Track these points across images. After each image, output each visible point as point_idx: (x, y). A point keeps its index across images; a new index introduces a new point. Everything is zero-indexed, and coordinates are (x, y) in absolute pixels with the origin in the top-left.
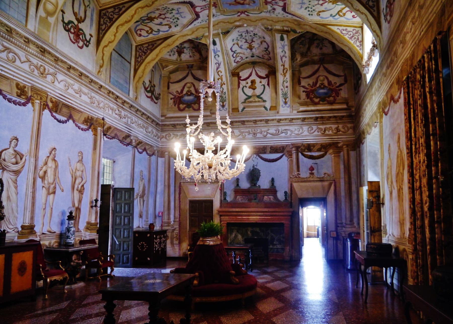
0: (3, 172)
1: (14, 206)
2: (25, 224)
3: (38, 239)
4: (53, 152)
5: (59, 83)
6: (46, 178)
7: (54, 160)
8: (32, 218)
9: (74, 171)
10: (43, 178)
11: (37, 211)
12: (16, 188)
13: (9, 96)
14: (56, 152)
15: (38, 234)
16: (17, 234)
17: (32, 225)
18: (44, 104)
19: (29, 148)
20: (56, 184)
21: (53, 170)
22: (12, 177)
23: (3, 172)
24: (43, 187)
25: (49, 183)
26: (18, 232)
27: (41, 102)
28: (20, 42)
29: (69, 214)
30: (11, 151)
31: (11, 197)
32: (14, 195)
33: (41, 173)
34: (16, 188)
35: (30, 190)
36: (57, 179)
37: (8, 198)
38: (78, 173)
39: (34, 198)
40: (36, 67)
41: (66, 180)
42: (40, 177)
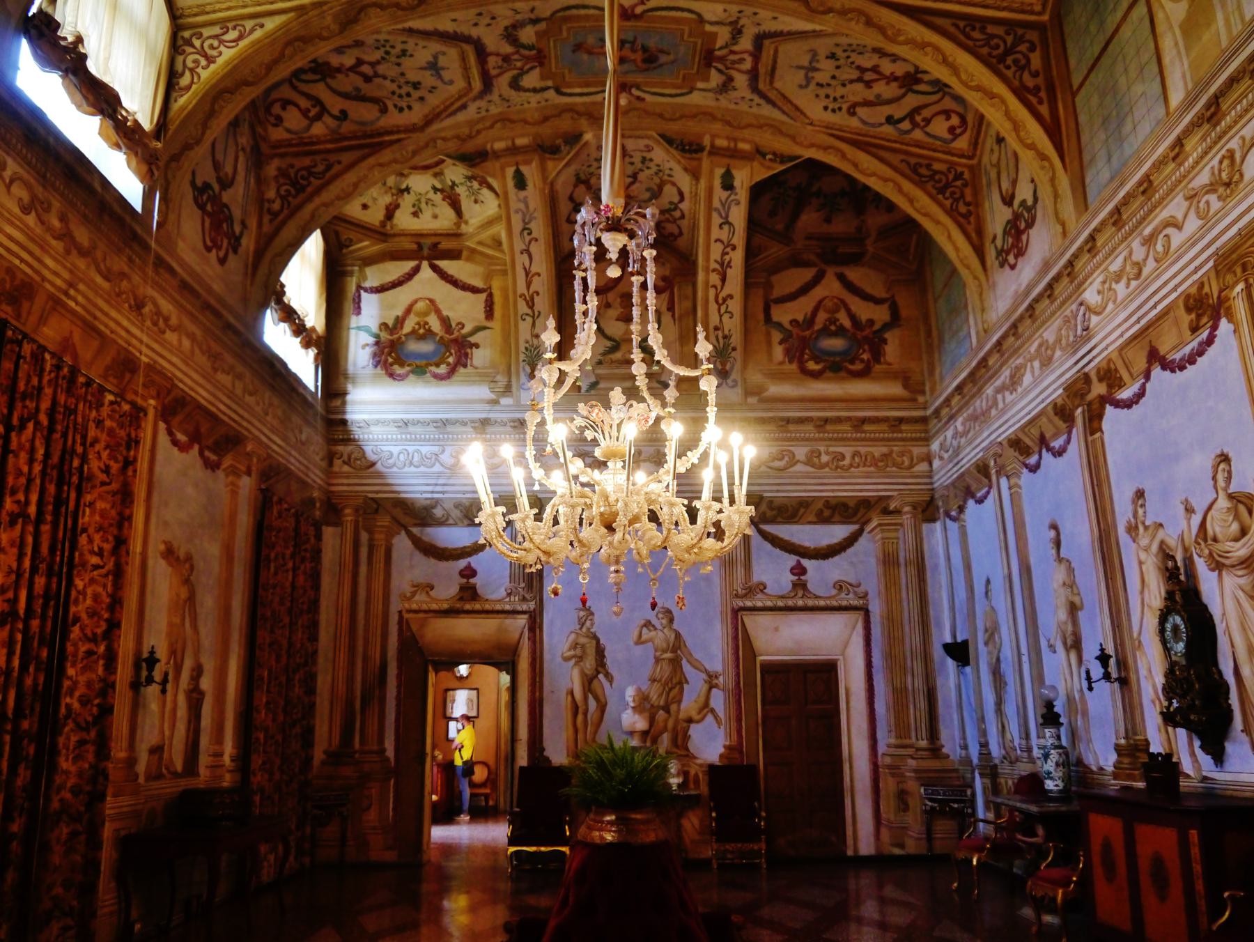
0: (1220, 575)
22: (1242, 581)
23: (1220, 575)
28: (1169, 177)
30: (1223, 503)
40: (1211, 188)
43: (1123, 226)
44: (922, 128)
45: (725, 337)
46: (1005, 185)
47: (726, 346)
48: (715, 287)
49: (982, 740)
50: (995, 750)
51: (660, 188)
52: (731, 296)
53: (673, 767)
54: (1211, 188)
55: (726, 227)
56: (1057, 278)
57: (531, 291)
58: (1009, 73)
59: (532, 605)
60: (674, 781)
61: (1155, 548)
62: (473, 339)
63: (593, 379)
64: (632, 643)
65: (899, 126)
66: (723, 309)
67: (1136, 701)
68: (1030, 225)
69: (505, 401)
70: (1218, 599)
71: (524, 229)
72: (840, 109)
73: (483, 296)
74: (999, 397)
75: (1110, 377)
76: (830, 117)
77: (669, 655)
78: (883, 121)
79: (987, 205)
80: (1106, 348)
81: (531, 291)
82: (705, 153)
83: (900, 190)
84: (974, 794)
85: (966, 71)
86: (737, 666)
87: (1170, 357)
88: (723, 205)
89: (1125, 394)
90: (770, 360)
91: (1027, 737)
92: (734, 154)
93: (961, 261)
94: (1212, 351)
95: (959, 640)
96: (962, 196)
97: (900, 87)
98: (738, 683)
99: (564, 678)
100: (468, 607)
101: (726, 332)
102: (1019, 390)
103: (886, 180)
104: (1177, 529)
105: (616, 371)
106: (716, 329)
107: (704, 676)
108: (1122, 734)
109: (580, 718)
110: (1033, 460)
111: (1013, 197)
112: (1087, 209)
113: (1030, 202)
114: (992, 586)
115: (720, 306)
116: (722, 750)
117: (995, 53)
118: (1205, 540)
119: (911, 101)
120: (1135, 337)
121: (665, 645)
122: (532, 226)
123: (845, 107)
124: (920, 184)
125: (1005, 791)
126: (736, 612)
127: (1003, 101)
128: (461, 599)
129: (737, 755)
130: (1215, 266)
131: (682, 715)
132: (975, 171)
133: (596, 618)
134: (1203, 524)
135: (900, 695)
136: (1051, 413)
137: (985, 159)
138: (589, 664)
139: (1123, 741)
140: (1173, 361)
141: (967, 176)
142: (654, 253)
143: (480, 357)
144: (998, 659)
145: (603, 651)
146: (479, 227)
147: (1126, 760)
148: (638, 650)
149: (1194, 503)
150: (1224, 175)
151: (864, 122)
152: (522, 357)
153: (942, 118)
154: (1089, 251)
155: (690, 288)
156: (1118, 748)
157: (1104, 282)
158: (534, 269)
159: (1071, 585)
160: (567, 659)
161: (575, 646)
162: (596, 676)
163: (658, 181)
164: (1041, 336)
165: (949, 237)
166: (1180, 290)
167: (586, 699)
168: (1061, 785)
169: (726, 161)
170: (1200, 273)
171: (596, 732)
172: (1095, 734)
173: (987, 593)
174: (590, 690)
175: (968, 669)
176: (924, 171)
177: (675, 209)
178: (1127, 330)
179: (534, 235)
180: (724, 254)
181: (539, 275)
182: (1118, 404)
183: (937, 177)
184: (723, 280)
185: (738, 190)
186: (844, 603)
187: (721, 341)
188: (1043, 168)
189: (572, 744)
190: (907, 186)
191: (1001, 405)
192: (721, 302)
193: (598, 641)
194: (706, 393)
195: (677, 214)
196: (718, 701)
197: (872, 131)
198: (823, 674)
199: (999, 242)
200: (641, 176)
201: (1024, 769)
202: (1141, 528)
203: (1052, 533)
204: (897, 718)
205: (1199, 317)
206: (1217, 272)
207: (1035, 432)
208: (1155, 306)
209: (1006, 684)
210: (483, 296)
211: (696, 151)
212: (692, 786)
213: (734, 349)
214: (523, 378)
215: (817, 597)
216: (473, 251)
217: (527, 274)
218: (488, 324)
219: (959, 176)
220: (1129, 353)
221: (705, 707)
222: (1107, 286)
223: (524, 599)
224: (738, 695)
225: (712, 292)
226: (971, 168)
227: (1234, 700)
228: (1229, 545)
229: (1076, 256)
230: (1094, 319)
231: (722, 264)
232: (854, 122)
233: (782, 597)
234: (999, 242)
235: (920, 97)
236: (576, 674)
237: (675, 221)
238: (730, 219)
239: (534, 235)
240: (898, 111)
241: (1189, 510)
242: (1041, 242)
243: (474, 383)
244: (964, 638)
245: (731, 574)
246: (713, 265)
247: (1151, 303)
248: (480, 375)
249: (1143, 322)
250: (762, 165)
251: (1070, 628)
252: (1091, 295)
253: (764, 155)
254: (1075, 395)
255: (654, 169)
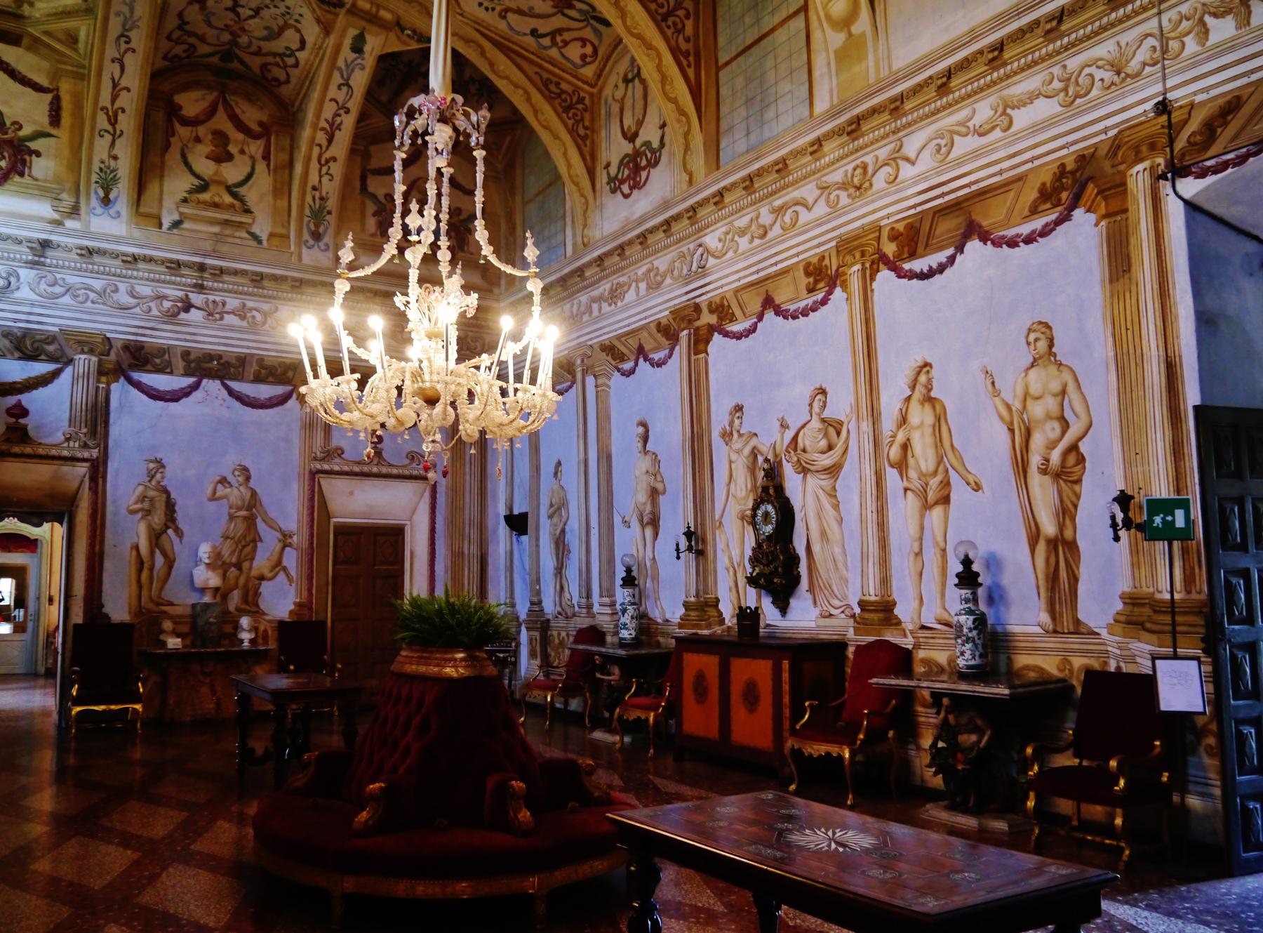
0: (805, 478)
1: (837, 551)
2: (867, 598)
3: (907, 642)
4: (923, 378)
5: (913, 163)
6: (911, 461)
7: (929, 400)
8: (885, 581)
9: (1017, 405)
10: (901, 466)
11: (895, 560)
12: (836, 507)
13: (792, 308)
14: (934, 373)
15: (909, 626)
16: (851, 621)
17: (888, 602)
18: (873, 263)
19: (851, 398)
20: (947, 471)
21: (929, 431)
22: (823, 483)
23: (805, 478)
24: (906, 490)
25: (922, 475)
26: (853, 616)
27: (863, 264)
28: (805, 166)
29: (960, 568)
30: (816, 424)
31: (828, 531)
32: (834, 525)
33: (895, 452)
34: (836, 507)
35: (871, 505)
36: (950, 454)
37: (823, 534)
38: (1037, 410)
39: (882, 525)
40: (843, 186)
41: (986, 446)
42: (892, 466)
43: (754, 192)
44: (559, 48)
45: (322, 199)
46: (628, 122)
47: (322, 208)
48: (320, 146)
49: (535, 599)
50: (549, 606)
51: (282, 30)
52: (334, 159)
53: (245, 622)
54: (843, 186)
55: (345, 89)
56: (676, 218)
57: (116, 106)
58: (669, 32)
59: (95, 453)
60: (246, 636)
61: (747, 451)
62: (33, 145)
63: (176, 217)
64: (205, 499)
65: (541, 40)
66: (324, 170)
67: (711, 567)
68: (653, 163)
69: (70, 224)
70: (800, 495)
71: (122, 35)
72: (493, 9)
73: (49, 97)
74: (595, 306)
75: (722, 310)
76: (481, 14)
77: (243, 513)
78: (528, 31)
79: (603, 134)
80: (721, 287)
81: (116, 106)
82: (343, 11)
83: (529, 99)
84: (518, 645)
85: (633, 18)
86: (312, 527)
87: (784, 307)
88: (347, 66)
89: (736, 328)
90: (363, 229)
91: (589, 596)
92: (373, 19)
93: (570, 176)
94: (824, 309)
95: (516, 512)
96: (582, 120)
97: (554, 7)
98: (311, 543)
99: (129, 532)
100: (16, 449)
101: (324, 194)
102: (619, 304)
103: (517, 86)
104: (770, 439)
105: (204, 213)
106: (314, 188)
107: (278, 535)
108: (693, 592)
109: (145, 574)
110: (627, 366)
111: (636, 135)
112: (718, 168)
113: (655, 144)
114: (563, 468)
115: (321, 165)
116: (292, 607)
117: (660, 11)
118: (795, 450)
119: (559, 21)
120: (752, 284)
121: (240, 503)
122: (133, 34)
123: (498, 8)
124: (549, 99)
125: (557, 641)
126: (313, 474)
127: (659, 55)
128: (8, 440)
129: (305, 612)
130: (837, 247)
131: (254, 573)
132: (596, 99)
133: (169, 471)
134: (795, 438)
135: (457, 557)
136: (654, 330)
137: (608, 92)
138: (158, 519)
139: (693, 599)
140: (787, 311)
141: (587, 101)
142: (484, 153)
143: (42, 167)
144: (563, 531)
145: (174, 505)
146: (49, 15)
147: (693, 614)
148: (212, 506)
149: (789, 420)
150: (856, 180)
151: (511, 28)
152: (94, 177)
153: (578, 44)
154: (715, 204)
155: (288, 142)
156: (687, 605)
157: (727, 233)
158: (123, 83)
159: (655, 473)
160: (133, 512)
161: (142, 498)
162: (165, 532)
163: (281, 22)
164: (651, 263)
165: (565, 154)
166: (801, 257)
167: (152, 553)
168: (634, 634)
169: (364, 24)
170: (822, 249)
171: (161, 589)
172: (665, 595)
173: (556, 474)
174: (158, 546)
175: (524, 538)
176: (552, 87)
177: (290, 56)
178: (745, 277)
179: (132, 45)
180: (337, 115)
181: (129, 90)
182: (726, 334)
183: (563, 96)
184: (330, 141)
185: (366, 55)
186: (415, 473)
187: (317, 201)
188: (679, 121)
189: (134, 602)
190: (537, 97)
191: (596, 313)
192: (324, 163)
193: (168, 494)
194: (531, 294)
195: (291, 61)
196: (291, 560)
197: (516, 38)
198: (395, 535)
199: (613, 170)
200: (265, 13)
201: (583, 622)
202: (735, 435)
203: (641, 430)
204: (453, 579)
205: (816, 282)
206: (838, 252)
207: (634, 343)
208: (776, 264)
209: (569, 552)
210: (49, 97)
211: (335, 6)
212: (260, 641)
213: (329, 213)
214: (94, 202)
215: (391, 465)
216: (36, 40)
217: (115, 85)
218: (53, 132)
219: (581, 100)
220: (745, 296)
221: (278, 565)
222: (730, 236)
223: (85, 446)
224: (311, 556)
225: (316, 150)
226: (591, 95)
227: (803, 568)
228: (816, 456)
229: (701, 204)
230: (712, 261)
231: (332, 125)
232: (502, 25)
233: (359, 463)
234: (613, 170)
235: (566, 20)
236: (142, 528)
237: (285, 66)
238: (351, 83)
239: (132, 45)
240: (544, 27)
241: (784, 426)
242: (661, 184)
243: (32, 196)
244: (523, 510)
245: (311, 437)
246: (323, 124)
247: (773, 261)
248: (39, 188)
249: (762, 274)
250: (398, 37)
251: (648, 508)
252: (712, 240)
253: (403, 29)
254: (682, 319)
255: (283, 9)
